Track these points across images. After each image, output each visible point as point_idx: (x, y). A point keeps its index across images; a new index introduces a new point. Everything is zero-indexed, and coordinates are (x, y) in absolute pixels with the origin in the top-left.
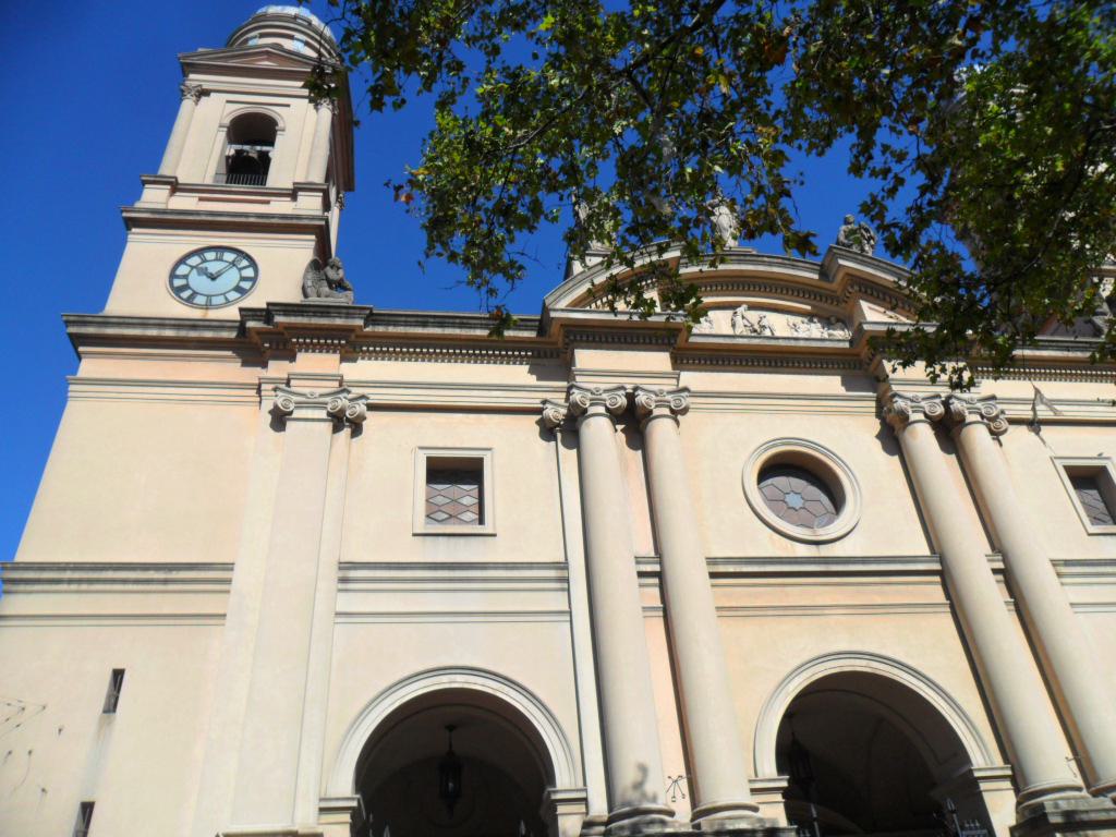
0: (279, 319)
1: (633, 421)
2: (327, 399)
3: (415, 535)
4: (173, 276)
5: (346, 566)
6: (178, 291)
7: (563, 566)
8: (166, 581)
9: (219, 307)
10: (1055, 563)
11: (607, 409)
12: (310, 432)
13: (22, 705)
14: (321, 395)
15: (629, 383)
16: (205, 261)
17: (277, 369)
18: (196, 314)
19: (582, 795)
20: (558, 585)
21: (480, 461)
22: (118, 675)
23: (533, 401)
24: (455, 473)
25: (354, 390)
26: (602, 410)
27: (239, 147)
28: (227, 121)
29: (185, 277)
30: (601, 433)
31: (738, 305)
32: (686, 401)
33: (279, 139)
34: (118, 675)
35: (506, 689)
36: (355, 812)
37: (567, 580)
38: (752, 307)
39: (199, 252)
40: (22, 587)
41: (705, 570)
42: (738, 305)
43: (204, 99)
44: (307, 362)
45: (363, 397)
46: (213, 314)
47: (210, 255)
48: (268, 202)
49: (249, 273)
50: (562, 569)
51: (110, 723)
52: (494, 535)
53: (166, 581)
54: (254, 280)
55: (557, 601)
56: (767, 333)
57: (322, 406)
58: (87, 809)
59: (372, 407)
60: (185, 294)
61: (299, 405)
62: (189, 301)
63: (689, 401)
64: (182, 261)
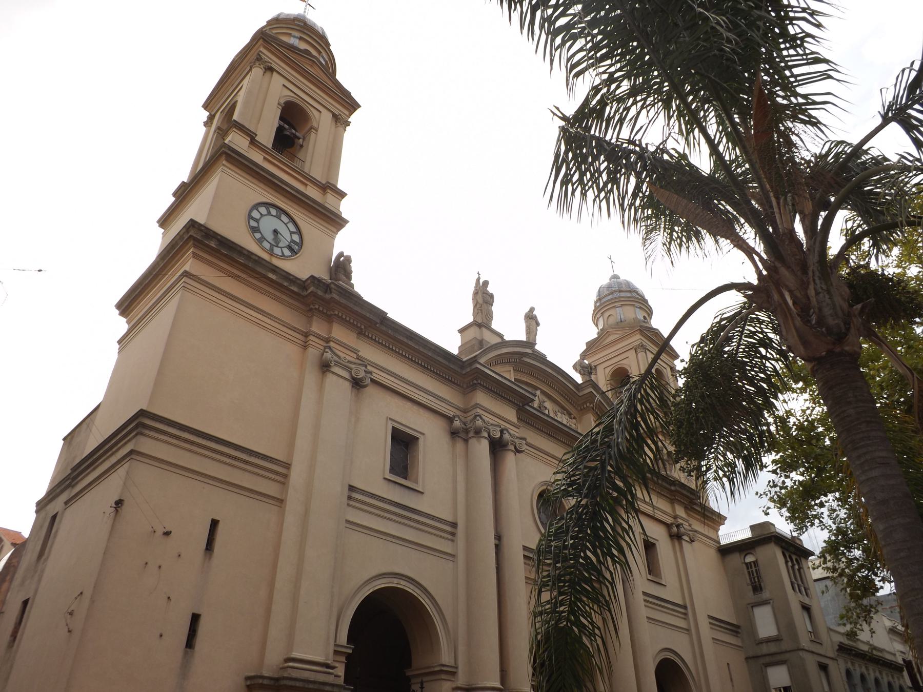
0: (334, 296)
1: (497, 447)
2: (352, 366)
3: (385, 479)
4: (250, 217)
5: (352, 488)
6: (255, 230)
7: (454, 525)
8: (247, 462)
9: (278, 257)
10: (644, 593)
11: (489, 435)
12: (337, 387)
13: (160, 531)
14: (349, 362)
15: (504, 425)
16: (269, 214)
17: (318, 327)
18: (265, 256)
19: (454, 670)
20: (450, 537)
21: (417, 439)
22: (214, 524)
23: (451, 412)
24: (403, 444)
25: (369, 368)
26: (486, 435)
27: (282, 123)
28: (282, 101)
29: (257, 221)
30: (482, 448)
31: (536, 388)
32: (525, 447)
33: (313, 135)
34: (214, 524)
35: (424, 596)
36: (348, 656)
37: (453, 534)
38: (543, 392)
39: (268, 205)
40: (152, 433)
41: (521, 553)
42: (536, 388)
43: (268, 74)
44: (339, 333)
45: (371, 373)
46: (276, 262)
47: (273, 211)
48: (306, 185)
49: (296, 238)
50: (452, 527)
51: (210, 558)
52: (422, 493)
53: (247, 462)
54: (301, 244)
55: (446, 546)
56: (546, 412)
57: (349, 370)
58: (195, 618)
59: (373, 381)
60: (258, 235)
61: (338, 364)
62: (260, 241)
63: (525, 447)
64: (256, 206)
